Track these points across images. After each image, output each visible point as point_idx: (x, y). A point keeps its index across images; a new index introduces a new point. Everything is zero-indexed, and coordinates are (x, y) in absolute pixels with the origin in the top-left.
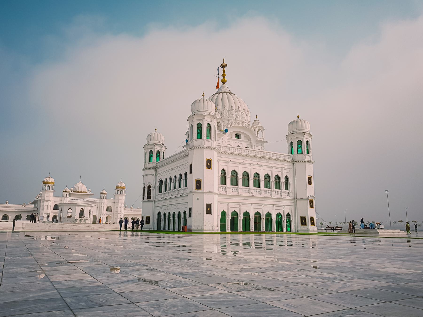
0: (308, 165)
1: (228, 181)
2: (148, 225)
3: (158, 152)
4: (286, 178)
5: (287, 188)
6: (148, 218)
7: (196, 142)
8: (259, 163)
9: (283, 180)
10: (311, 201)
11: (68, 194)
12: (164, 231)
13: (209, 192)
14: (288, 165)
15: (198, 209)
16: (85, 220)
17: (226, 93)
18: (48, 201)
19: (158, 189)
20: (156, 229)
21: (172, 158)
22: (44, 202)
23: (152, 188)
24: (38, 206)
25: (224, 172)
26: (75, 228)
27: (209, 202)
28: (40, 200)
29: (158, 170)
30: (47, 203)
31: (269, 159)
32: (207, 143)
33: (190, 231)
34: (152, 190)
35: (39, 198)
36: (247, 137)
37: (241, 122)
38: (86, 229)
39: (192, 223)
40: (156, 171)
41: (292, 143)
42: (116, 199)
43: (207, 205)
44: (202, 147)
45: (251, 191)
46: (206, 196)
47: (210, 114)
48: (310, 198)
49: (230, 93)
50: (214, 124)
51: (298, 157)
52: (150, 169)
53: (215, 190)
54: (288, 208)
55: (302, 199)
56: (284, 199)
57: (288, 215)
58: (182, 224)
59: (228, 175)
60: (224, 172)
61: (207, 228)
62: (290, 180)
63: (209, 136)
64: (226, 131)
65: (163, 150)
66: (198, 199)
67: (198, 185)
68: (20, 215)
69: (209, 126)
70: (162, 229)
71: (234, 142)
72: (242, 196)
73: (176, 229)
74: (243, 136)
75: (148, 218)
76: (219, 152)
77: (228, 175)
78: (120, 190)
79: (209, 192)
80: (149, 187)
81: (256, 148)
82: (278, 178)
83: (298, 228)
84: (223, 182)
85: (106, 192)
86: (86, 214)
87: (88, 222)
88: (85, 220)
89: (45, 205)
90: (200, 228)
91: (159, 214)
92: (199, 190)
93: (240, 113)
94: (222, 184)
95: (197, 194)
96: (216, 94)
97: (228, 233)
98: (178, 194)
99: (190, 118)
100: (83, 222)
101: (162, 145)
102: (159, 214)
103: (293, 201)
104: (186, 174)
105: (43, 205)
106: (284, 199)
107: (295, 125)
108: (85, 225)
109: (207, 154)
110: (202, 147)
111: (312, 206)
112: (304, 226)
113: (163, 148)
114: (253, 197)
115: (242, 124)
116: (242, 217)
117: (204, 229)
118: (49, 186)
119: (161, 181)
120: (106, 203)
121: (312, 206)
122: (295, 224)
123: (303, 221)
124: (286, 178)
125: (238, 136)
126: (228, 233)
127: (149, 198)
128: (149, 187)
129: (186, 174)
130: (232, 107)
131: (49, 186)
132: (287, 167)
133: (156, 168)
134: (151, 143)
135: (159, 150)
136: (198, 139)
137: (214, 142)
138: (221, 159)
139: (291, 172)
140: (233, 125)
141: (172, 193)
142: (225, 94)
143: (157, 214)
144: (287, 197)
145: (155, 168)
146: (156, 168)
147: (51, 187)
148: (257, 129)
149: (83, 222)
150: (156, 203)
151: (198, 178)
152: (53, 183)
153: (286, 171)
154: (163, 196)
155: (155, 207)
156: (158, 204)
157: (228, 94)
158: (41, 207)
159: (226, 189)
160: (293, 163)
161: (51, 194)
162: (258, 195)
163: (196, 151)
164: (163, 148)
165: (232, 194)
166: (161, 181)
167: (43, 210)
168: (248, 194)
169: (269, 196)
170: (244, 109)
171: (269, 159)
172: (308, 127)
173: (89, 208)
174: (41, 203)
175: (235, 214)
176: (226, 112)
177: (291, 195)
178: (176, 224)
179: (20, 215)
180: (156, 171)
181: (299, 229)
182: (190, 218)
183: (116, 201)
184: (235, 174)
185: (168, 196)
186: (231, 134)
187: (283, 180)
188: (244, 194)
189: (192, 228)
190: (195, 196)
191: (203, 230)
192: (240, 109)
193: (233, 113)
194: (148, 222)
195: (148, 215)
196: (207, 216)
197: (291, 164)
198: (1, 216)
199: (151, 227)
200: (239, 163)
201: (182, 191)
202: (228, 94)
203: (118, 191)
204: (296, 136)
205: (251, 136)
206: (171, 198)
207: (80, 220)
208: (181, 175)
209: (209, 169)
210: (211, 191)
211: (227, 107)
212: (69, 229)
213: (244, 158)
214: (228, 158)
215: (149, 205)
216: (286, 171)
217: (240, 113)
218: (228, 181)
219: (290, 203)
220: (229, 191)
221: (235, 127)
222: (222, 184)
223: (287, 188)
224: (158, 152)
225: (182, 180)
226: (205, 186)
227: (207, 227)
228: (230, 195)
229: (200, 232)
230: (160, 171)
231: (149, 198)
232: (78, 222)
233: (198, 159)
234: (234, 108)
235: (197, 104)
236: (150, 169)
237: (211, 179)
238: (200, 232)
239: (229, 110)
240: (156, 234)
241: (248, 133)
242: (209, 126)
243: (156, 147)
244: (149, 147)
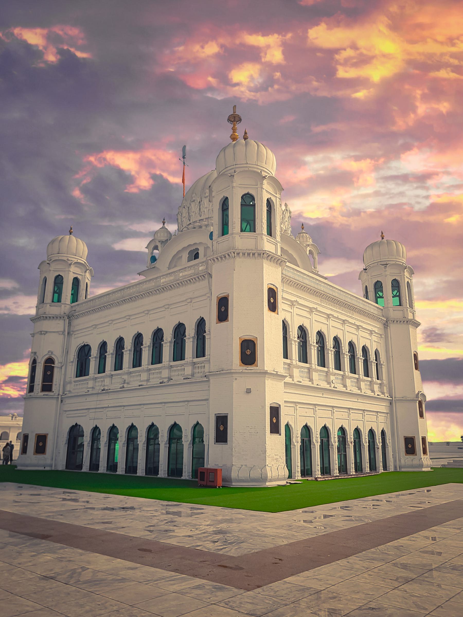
2: (40, 456)
14: (376, 327)
19: (72, 369)
21: (105, 299)
23: (56, 364)
29: (75, 322)
34: (56, 370)
40: (70, 324)
43: (271, 407)
44: (262, 255)
45: (332, 378)
55: (404, 400)
61: (275, 474)
66: (248, 391)
67: (248, 352)
80: (50, 361)
83: (400, 461)
90: (255, 474)
92: (250, 367)
95: (242, 379)
98: (148, 380)
103: (388, 404)
104: (201, 324)
109: (271, 275)
112: (411, 457)
117: (269, 475)
122: (394, 451)
123: (410, 445)
127: (47, 387)
128: (50, 361)
129: (201, 324)
133: (70, 317)
134: (60, 258)
135: (79, 277)
136: (243, 234)
139: (382, 341)
141: (125, 377)
143: (67, 430)
145: (69, 317)
146: (70, 317)
150: (67, 401)
151: (248, 334)
156: (70, 404)
159: (289, 369)
160: (386, 325)
163: (241, 264)
181: (403, 462)
182: (220, 446)
185: (116, 384)
189: (234, 475)
190: (239, 384)
191: (265, 479)
194: (41, 448)
199: (49, 462)
201: (167, 371)
204: (389, 271)
208: (138, 338)
219: (383, 407)
225: (183, 343)
230: (80, 323)
243: (73, 269)
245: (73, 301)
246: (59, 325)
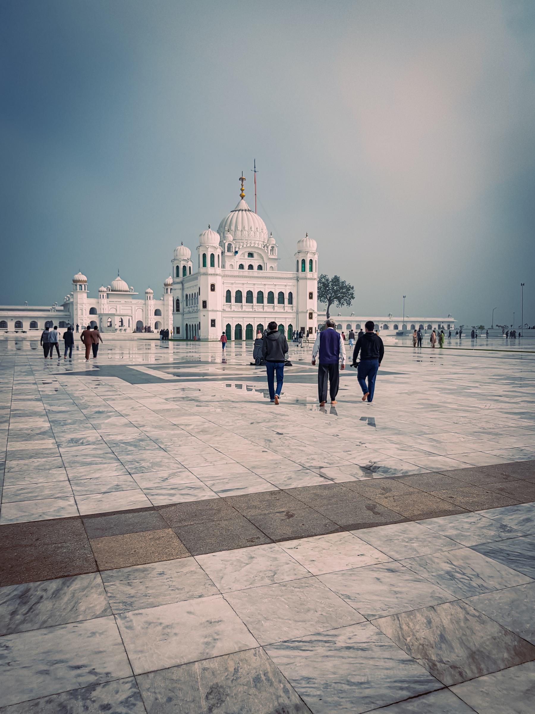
0: (309, 282)
1: (233, 299)
3: (184, 267)
4: (291, 294)
5: (291, 302)
6: (178, 329)
7: (203, 270)
8: (263, 283)
9: (286, 296)
10: (311, 315)
11: (105, 294)
12: (190, 340)
13: (213, 311)
15: (205, 323)
16: (125, 330)
17: (242, 210)
18: (82, 304)
20: (185, 338)
22: (77, 305)
24: (70, 310)
25: (229, 292)
26: (116, 338)
27: (213, 318)
28: (72, 303)
30: (81, 306)
31: (273, 278)
32: (210, 270)
33: (199, 340)
35: (71, 300)
36: (260, 255)
37: (253, 242)
38: (126, 338)
39: (202, 334)
40: (183, 285)
41: (298, 261)
42: (165, 299)
44: (206, 274)
46: (210, 313)
47: (214, 245)
48: (308, 312)
49: (246, 210)
50: (218, 252)
51: (301, 274)
52: (178, 283)
53: (220, 308)
54: (290, 320)
55: (302, 312)
56: (287, 312)
57: (290, 326)
58: (194, 335)
59: (233, 295)
60: (229, 292)
61: (212, 338)
62: (294, 296)
63: (212, 265)
64: (236, 252)
65: (190, 264)
68: (51, 321)
69: (212, 256)
70: (189, 338)
71: (246, 261)
72: (245, 312)
73: (192, 338)
74: (255, 255)
75: (178, 329)
76: (224, 276)
77: (233, 295)
78: (169, 287)
79: (213, 311)
80: (178, 300)
81: (269, 266)
82: (281, 294)
84: (228, 300)
85: (152, 291)
86: (126, 323)
87: (128, 331)
88: (125, 330)
89: (79, 309)
91: (187, 324)
93: (252, 233)
94: (227, 302)
96: (233, 211)
97: (244, 341)
99: (198, 248)
100: (123, 332)
101: (187, 261)
102: (187, 324)
103: (295, 314)
105: (77, 309)
106: (287, 312)
107: (301, 244)
108: (125, 335)
109: (211, 280)
110: (206, 274)
111: (311, 318)
113: (190, 263)
114: (255, 312)
115: (255, 243)
116: (245, 329)
117: (209, 338)
118: (81, 285)
119: (187, 295)
120: (153, 304)
121: (311, 318)
124: (291, 294)
125: (251, 255)
126: (244, 341)
127: (178, 310)
128: (178, 300)
130: (244, 228)
131: (81, 285)
132: (291, 284)
133: (182, 283)
137: (218, 270)
138: (225, 281)
139: (295, 288)
140: (245, 246)
142: (241, 212)
144: (291, 311)
147: (83, 286)
148: (270, 248)
149: (123, 332)
151: (204, 300)
152: (85, 282)
153: (290, 288)
154: (188, 309)
155: (183, 319)
156: (186, 316)
157: (244, 212)
158: (75, 312)
161: (85, 295)
162: (262, 310)
164: (190, 263)
165: (236, 310)
166: (187, 295)
167: (77, 315)
168: (251, 310)
169: (272, 310)
170: (257, 229)
171: (273, 278)
172: (312, 245)
173: (128, 317)
174: (75, 307)
175: (239, 327)
176: (239, 233)
177: (294, 308)
178: (190, 334)
179: (51, 321)
180: (183, 285)
183: (166, 303)
184: (239, 294)
186: (243, 254)
187: (286, 296)
188: (247, 310)
189: (201, 338)
190: (202, 314)
192: (253, 229)
193: (245, 233)
194: (178, 332)
195: (178, 326)
196: (211, 329)
197: (296, 281)
198: (29, 324)
200: (243, 284)
202: (244, 212)
203: (167, 289)
205: (263, 255)
206: (193, 312)
207: (120, 330)
209: (213, 292)
210: (215, 309)
211: (240, 228)
212: (110, 338)
213: (248, 279)
214: (232, 280)
215: (179, 317)
216: (290, 288)
217: (252, 233)
218: (233, 299)
220: (233, 308)
221: (247, 247)
222: (227, 302)
223: (291, 302)
224: (184, 267)
226: (209, 306)
227: (211, 337)
228: (234, 311)
229: (206, 340)
230: (186, 285)
231: (178, 310)
232: (118, 331)
233: (204, 283)
234: (246, 229)
235: (202, 236)
236: (178, 283)
237: (216, 300)
238: (206, 340)
239: (242, 231)
240: (185, 343)
241: (260, 252)
242: (212, 256)
244: (176, 262)
245: (184, 276)
246: (180, 286)
